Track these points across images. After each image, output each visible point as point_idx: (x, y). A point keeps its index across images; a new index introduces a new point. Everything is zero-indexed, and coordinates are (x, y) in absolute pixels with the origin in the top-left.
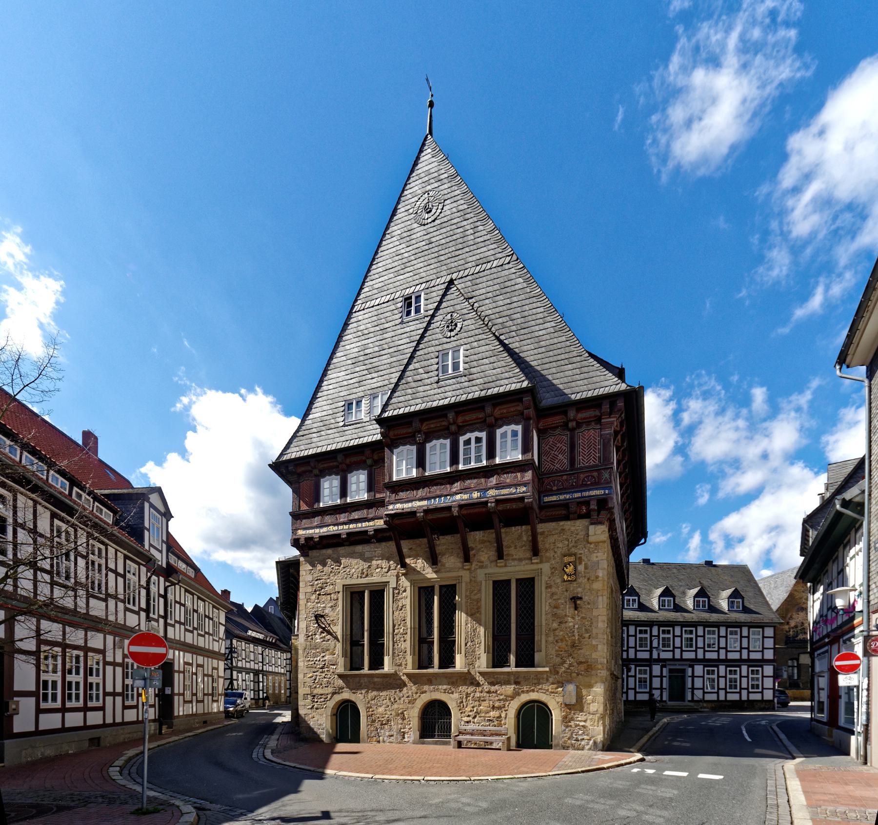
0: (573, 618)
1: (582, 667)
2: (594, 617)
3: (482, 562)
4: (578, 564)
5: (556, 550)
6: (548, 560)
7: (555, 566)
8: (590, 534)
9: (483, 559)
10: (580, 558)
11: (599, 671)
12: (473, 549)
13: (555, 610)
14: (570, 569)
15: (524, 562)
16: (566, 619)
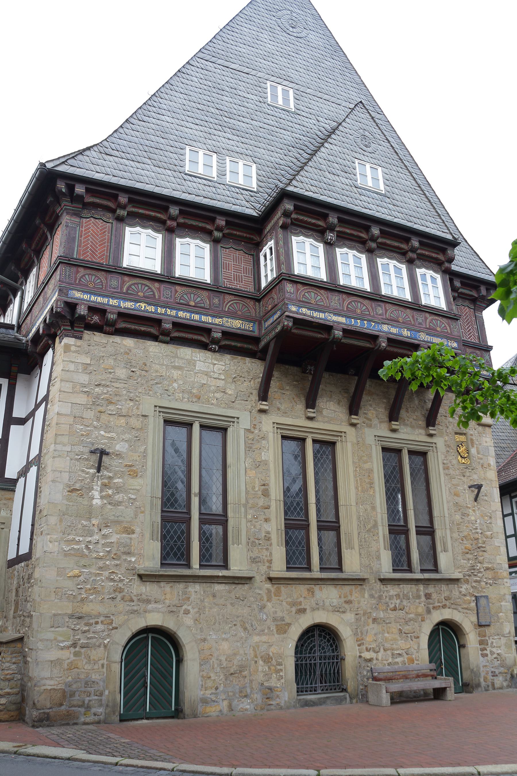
3: (370, 420)
4: (470, 446)
7: (448, 443)
10: (472, 440)
11: (505, 580)
13: (455, 497)
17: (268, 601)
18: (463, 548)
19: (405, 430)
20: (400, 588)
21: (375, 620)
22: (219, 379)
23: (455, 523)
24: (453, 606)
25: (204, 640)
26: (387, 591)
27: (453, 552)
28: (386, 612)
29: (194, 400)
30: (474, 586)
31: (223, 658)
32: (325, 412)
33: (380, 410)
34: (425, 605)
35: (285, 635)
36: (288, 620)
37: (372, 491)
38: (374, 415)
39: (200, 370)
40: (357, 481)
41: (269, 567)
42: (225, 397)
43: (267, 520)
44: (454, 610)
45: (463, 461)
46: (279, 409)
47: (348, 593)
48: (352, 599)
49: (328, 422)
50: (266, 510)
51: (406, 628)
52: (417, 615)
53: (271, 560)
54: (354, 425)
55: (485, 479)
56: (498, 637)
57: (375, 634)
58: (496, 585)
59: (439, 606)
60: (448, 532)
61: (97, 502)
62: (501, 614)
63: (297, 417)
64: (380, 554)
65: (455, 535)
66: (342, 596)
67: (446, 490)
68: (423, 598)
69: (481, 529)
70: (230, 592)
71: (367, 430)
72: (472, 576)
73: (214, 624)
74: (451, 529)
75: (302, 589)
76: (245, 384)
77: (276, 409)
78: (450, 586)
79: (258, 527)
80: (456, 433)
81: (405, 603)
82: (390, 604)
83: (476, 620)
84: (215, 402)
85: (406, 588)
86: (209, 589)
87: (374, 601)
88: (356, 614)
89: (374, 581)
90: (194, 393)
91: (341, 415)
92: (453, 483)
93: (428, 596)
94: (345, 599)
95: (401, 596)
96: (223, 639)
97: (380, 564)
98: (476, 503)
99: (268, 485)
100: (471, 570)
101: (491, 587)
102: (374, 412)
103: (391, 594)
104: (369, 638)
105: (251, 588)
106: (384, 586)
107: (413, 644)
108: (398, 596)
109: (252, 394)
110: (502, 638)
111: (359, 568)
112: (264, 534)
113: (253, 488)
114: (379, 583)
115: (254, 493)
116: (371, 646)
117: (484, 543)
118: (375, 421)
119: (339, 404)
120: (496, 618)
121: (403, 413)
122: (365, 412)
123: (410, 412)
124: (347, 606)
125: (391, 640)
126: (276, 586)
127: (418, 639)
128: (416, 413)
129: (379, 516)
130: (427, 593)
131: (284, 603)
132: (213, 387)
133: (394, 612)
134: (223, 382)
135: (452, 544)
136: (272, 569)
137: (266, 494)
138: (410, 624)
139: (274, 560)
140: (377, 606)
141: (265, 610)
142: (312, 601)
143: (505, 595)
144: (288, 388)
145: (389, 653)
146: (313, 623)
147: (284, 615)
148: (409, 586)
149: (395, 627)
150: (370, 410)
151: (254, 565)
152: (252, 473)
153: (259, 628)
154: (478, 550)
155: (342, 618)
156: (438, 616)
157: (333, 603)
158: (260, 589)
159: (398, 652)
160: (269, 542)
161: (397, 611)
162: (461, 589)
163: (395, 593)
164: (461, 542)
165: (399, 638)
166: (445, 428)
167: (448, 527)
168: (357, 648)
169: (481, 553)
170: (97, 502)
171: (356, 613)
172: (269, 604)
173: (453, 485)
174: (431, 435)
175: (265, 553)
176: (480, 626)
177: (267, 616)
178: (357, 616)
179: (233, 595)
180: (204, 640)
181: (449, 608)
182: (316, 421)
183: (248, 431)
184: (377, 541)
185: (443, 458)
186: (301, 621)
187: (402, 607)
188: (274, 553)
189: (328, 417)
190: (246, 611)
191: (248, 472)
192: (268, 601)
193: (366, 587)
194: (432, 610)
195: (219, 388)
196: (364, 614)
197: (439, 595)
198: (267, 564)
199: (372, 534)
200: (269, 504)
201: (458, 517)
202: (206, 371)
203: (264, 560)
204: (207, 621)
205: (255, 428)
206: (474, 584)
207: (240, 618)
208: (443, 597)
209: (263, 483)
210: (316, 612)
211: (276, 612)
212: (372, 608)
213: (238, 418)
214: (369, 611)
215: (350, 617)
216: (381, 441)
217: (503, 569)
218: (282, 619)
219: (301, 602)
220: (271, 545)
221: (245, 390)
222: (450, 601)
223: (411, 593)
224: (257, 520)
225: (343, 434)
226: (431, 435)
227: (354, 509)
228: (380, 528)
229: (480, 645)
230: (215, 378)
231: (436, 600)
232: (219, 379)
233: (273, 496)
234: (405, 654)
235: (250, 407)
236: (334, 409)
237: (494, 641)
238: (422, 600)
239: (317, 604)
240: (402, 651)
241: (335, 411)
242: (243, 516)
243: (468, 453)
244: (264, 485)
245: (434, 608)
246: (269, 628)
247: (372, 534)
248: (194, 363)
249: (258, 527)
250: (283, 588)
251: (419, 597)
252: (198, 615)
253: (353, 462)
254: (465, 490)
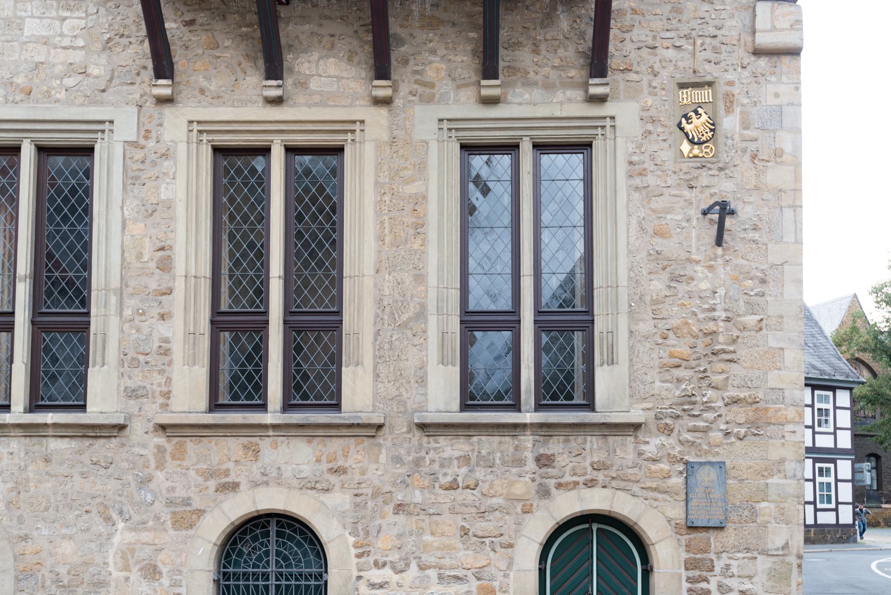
0: (711, 268)
1: (740, 414)
2: (772, 266)
3: (431, 85)
4: (722, 112)
5: (657, 67)
6: (634, 94)
7: (653, 112)
8: (759, 25)
9: (430, 74)
11: (789, 428)
12: (401, 42)
13: (657, 240)
14: (697, 125)
15: (560, 95)
16: (688, 272)
17: (157, 468)
18: (665, 355)
19: (527, 96)
20: (471, 444)
21: (400, 508)
22: (74, 48)
23: (648, 299)
24: (614, 484)
25: (25, 538)
26: (435, 449)
27: (631, 366)
28: (431, 493)
29: (18, 98)
30: (688, 442)
31: (63, 570)
32: (313, 85)
33: (459, 59)
34: (533, 480)
35: (191, 532)
36: (197, 504)
37: (420, 242)
38: (443, 73)
39: (33, 35)
40: (382, 223)
41: (165, 406)
42: (85, 83)
43: (162, 317)
44: (619, 493)
45: (696, 151)
46: (202, 91)
47: (340, 453)
48: (347, 465)
49: (322, 104)
50: (164, 298)
51: (479, 526)
52: (512, 499)
53: (169, 392)
54: (385, 102)
55: (757, 188)
56: (749, 555)
57: (400, 536)
58: (758, 438)
59: (576, 483)
60: (623, 322)
62: (764, 504)
63: (244, 103)
64: (426, 373)
65: (645, 327)
66: (324, 458)
67: (628, 224)
68: (531, 465)
69: (726, 310)
70: (79, 452)
72: (686, 417)
73: (47, 509)
74: (631, 313)
75: (234, 446)
76: (130, 51)
77: (197, 93)
78: (611, 439)
79: (146, 331)
80: (682, 86)
81: (480, 474)
82: (440, 476)
83: (683, 516)
84: (62, 95)
85: (488, 444)
86: (36, 448)
87: (403, 470)
88: (356, 495)
89: (405, 430)
90: (18, 85)
91: (353, 85)
92: (653, 205)
93: (544, 461)
94: (330, 465)
95: (474, 460)
96: (64, 537)
97: (426, 394)
98: (719, 251)
99: (171, 248)
100: (682, 404)
101: (738, 443)
102: (443, 66)
103: (446, 455)
104: (381, 543)
105: (123, 445)
106: (431, 439)
107: (498, 559)
108: (465, 460)
109: (145, 68)
110: (760, 557)
111: (369, 402)
112: (156, 344)
113: (139, 256)
114: (418, 434)
115: (140, 265)
116: (388, 559)
117: (734, 341)
118: (445, 87)
119: (350, 60)
120: (746, 513)
121: (505, 58)
122: (416, 68)
123: (544, 52)
124: (333, 479)
125: (438, 549)
126: (176, 440)
127: (510, 550)
128: (561, 52)
129: (432, 295)
130: (541, 455)
131: (192, 473)
132: (60, 67)
133: (452, 492)
134: (83, 53)
135: (631, 348)
136: (170, 408)
137: (166, 265)
138: (491, 517)
139: (174, 393)
140: (409, 480)
141: (152, 485)
142: (254, 469)
143: (782, 461)
144: (227, 43)
145: (433, 574)
146: (254, 510)
147: (191, 495)
148: (497, 439)
149: (450, 523)
150: (431, 62)
151: (132, 402)
152: (136, 229)
153: (136, 518)
154: (715, 358)
155: (322, 503)
157: (300, 471)
158: (144, 446)
159: (454, 573)
160: (167, 359)
161: (459, 490)
162: (643, 447)
163: (457, 454)
164: (660, 341)
165: (460, 545)
166: (646, 79)
167: (624, 308)
168: (355, 560)
169: (720, 366)
171: (356, 492)
172: (160, 475)
173: (653, 211)
174: (601, 99)
175: (158, 379)
176: (692, 528)
177: (155, 495)
178: (358, 499)
179: (86, 458)
180: (25, 538)
181: (604, 487)
182: (291, 106)
183: (134, 144)
184: (422, 347)
185: (630, 150)
186: (226, 506)
187: (472, 483)
188: (175, 377)
189: (320, 93)
190: (113, 485)
191: (130, 226)
192: (157, 468)
193: (385, 439)
194: (553, 491)
195: (73, 67)
196: (376, 494)
197: (578, 459)
198: (161, 400)
199: (409, 333)
200: (170, 284)
201: (658, 286)
202: (44, 37)
203: (154, 392)
204: (32, 504)
205: (146, 138)
206: (689, 436)
207: (98, 500)
208: (587, 464)
209: (159, 245)
210: (262, 490)
211: (173, 489)
212: (394, 484)
213: (111, 122)
214: (388, 488)
215: (340, 499)
216: (457, 130)
217: (787, 400)
218: (187, 502)
219: (228, 470)
220: (170, 363)
221: (130, 62)
222: (606, 472)
223: (499, 455)
224: (143, 318)
225: (357, 127)
226: (601, 99)
227: (368, 283)
228: (433, 321)
229: (687, 569)
230: (65, 48)
231: (568, 469)
232: (74, 48)
233: (180, 267)
234: (472, 579)
235: (137, 96)
236: (336, 74)
237: (732, 562)
238: (527, 468)
239: (263, 474)
240: (465, 572)
241: (339, 78)
242: (113, 312)
243: (711, 130)
244: (162, 249)
245: (559, 486)
246: (157, 518)
247: (409, 333)
248: (19, 25)
249: (146, 331)
250: (191, 445)
251: (520, 462)
252: (14, 494)
253: (377, 183)
254: (688, 221)
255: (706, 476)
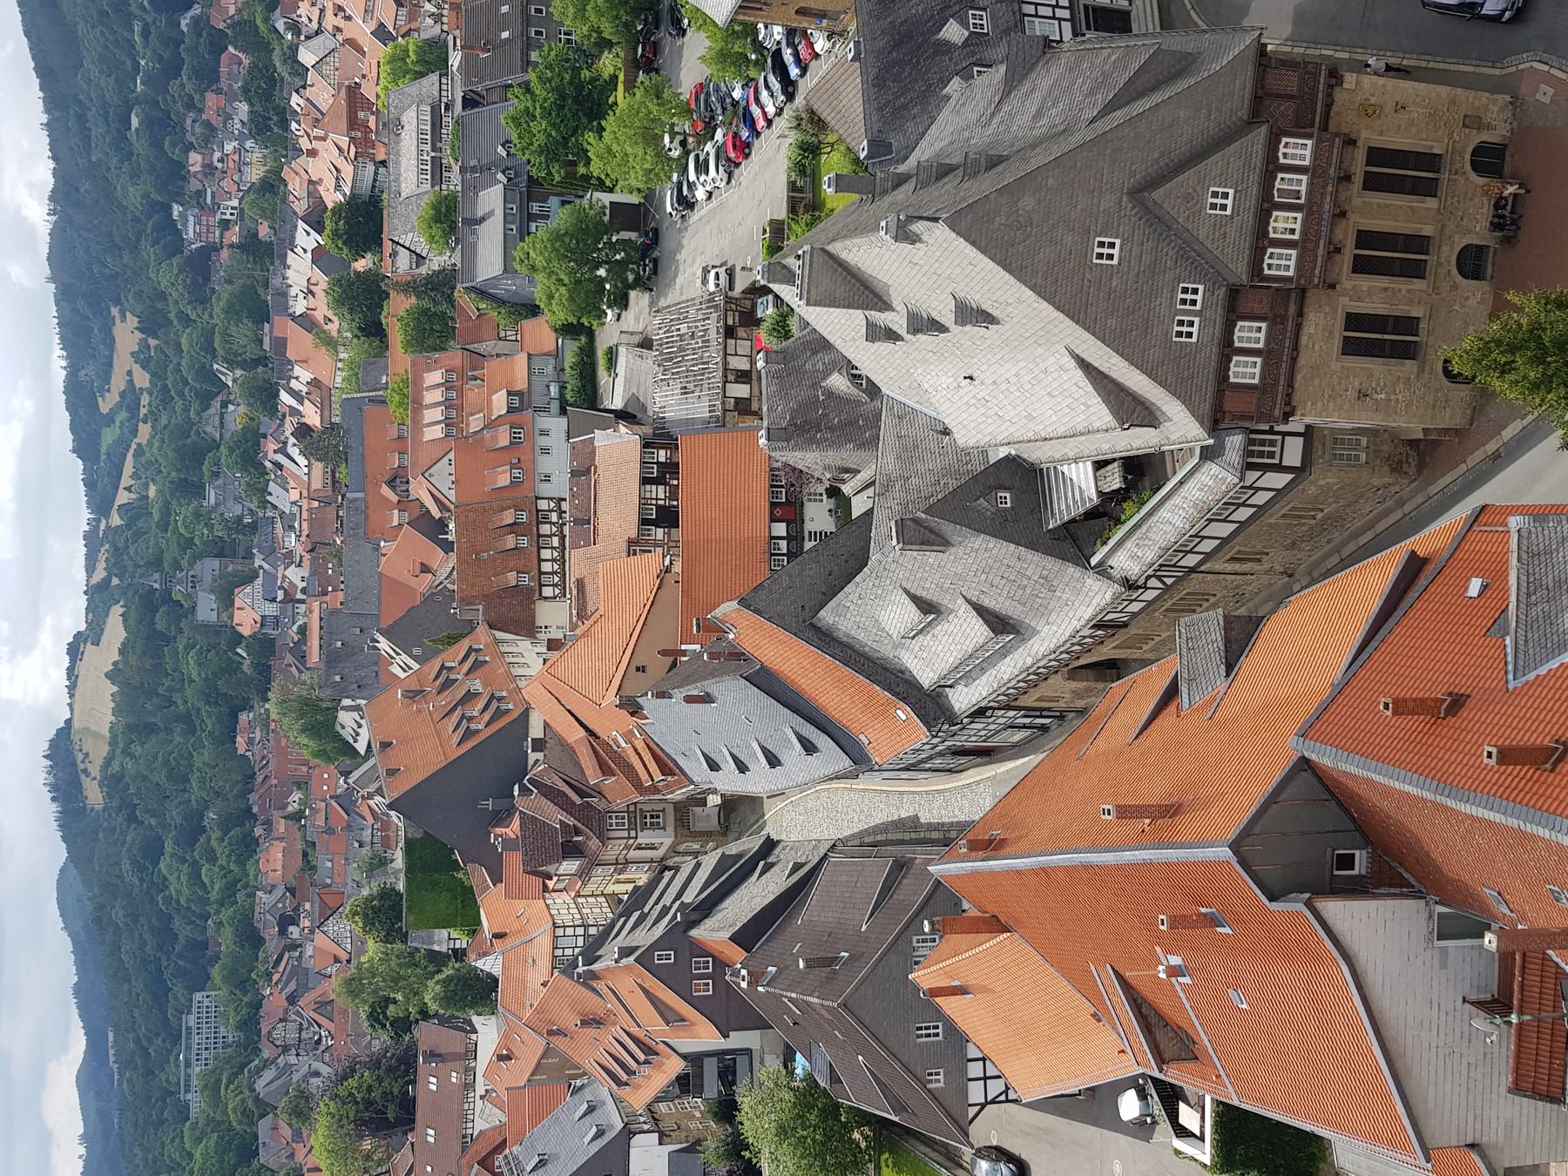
6: (1359, 131)
61: (1383, 396)
71: (1353, 203)
137: (1386, 289)
156: (1468, 167)
170: (1383, 396)
201: (1413, 130)
233: (1387, 285)
255: (1467, 121)
